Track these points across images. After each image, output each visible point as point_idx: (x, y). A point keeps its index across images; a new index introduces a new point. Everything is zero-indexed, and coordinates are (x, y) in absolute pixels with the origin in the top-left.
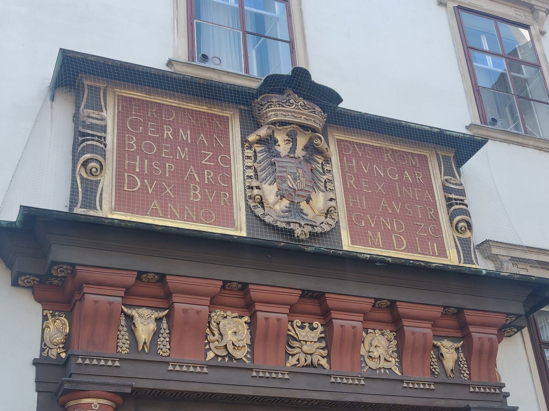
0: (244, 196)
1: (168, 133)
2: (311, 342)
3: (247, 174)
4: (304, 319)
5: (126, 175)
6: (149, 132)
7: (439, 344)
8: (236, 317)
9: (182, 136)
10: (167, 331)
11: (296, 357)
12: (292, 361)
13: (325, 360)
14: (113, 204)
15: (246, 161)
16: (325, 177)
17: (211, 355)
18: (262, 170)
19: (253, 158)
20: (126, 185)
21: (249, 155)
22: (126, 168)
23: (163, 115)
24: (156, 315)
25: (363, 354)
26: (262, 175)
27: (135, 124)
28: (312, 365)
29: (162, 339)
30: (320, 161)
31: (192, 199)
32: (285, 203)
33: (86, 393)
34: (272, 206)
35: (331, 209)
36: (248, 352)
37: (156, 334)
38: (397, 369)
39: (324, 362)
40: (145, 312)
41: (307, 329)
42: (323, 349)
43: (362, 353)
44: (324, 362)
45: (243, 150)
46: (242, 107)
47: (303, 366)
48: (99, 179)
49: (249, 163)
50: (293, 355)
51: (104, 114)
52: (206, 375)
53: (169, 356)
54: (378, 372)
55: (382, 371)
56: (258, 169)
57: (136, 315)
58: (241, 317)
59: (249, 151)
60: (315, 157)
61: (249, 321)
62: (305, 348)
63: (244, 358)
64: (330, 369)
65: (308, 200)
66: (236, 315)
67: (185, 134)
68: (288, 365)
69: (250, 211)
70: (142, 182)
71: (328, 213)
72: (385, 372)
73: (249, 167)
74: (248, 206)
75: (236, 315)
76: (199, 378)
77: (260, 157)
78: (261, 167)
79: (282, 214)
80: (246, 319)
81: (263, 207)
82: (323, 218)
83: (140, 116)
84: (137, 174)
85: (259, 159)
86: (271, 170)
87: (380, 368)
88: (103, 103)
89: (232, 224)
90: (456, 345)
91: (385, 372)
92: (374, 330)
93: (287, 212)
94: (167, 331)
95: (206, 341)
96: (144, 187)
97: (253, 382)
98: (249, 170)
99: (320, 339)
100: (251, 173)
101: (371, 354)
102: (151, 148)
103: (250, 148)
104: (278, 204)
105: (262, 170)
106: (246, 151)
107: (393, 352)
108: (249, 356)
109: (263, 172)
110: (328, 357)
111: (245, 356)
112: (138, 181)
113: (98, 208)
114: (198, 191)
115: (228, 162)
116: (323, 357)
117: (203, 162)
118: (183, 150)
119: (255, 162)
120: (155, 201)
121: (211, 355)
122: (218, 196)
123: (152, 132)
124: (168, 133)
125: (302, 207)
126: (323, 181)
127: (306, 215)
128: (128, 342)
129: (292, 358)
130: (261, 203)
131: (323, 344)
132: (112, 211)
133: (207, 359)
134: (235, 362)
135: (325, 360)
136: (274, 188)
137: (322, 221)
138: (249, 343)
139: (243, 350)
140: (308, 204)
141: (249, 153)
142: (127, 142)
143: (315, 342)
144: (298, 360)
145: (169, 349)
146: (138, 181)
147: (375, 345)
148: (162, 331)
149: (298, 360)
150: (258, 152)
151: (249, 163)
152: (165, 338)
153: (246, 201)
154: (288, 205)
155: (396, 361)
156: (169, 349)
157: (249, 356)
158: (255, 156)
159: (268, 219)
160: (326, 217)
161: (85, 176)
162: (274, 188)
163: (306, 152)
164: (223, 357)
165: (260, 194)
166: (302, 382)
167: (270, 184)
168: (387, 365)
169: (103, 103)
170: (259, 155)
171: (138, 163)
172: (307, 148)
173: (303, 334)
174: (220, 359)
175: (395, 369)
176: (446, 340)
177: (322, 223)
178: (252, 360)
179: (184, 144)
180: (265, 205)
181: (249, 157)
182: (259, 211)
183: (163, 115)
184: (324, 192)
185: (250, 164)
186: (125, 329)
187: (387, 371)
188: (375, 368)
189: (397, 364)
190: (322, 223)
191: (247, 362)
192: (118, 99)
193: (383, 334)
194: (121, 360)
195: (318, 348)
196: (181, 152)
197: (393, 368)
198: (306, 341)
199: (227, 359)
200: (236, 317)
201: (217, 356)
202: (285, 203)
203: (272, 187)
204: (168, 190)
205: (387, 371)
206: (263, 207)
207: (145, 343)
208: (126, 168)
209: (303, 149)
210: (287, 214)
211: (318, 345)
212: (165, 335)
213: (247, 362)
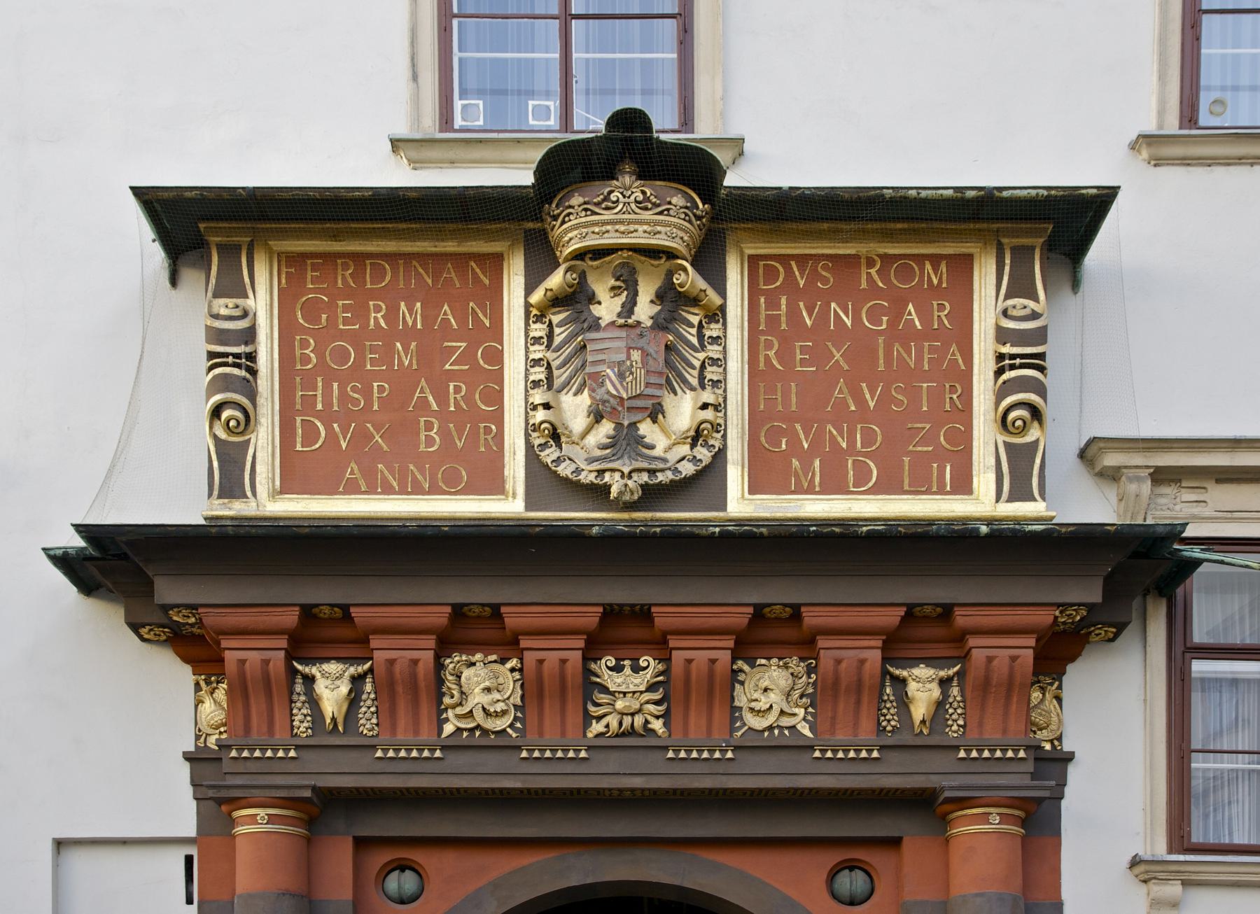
0: (523, 425)
1: (377, 318)
2: (634, 693)
3: (532, 378)
4: (620, 654)
5: (298, 419)
6: (340, 320)
7: (905, 673)
8: (495, 661)
9: (404, 318)
10: (372, 696)
11: (604, 721)
12: (597, 728)
13: (661, 721)
14: (278, 483)
15: (532, 348)
16: (702, 356)
17: (448, 729)
18: (559, 368)
19: (545, 340)
20: (299, 440)
21: (537, 334)
22: (298, 407)
23: (368, 279)
24: (352, 670)
25: (741, 705)
26: (560, 377)
27: (312, 311)
28: (632, 732)
29: (364, 709)
30: (695, 320)
31: (422, 448)
32: (606, 428)
33: (243, 802)
34: (576, 441)
35: (702, 426)
36: (516, 719)
37: (354, 700)
38: (807, 726)
39: (657, 725)
40: (333, 667)
41: (627, 671)
42: (657, 703)
43: (737, 703)
44: (657, 725)
45: (527, 324)
46: (530, 225)
47: (617, 736)
48: (247, 437)
49: (538, 352)
50: (599, 718)
51: (250, 302)
52: (441, 762)
53: (377, 735)
54: (766, 734)
55: (776, 732)
56: (554, 364)
57: (318, 675)
58: (503, 661)
59: (538, 325)
60: (683, 313)
61: (519, 665)
62: (620, 705)
63: (508, 730)
64: (670, 736)
65: (656, 413)
66: (494, 657)
67: (411, 310)
68: (590, 735)
69: (532, 455)
70: (329, 429)
71: (697, 437)
72: (781, 733)
73: (537, 362)
74: (529, 446)
75: (494, 657)
76: (429, 767)
77: (560, 335)
78: (562, 358)
79: (599, 453)
80: (514, 662)
81: (559, 446)
82: (685, 449)
83: (322, 291)
84: (318, 415)
85: (557, 340)
86: (577, 362)
87: (771, 728)
88: (247, 280)
89: (494, 484)
90: (942, 673)
91: (781, 733)
92: (769, 659)
93: (605, 447)
94: (372, 696)
95: (443, 707)
96: (331, 437)
97: (526, 768)
98: (537, 369)
99: (651, 688)
100: (539, 374)
101: (753, 705)
102: (343, 356)
103: (539, 319)
104: (593, 432)
105: (559, 368)
106: (533, 326)
107: (801, 697)
108: (518, 725)
109: (562, 370)
110: (666, 716)
111: (511, 726)
112: (321, 428)
113: (249, 494)
114: (435, 431)
115: (496, 357)
116: (657, 717)
117: (447, 367)
118: (406, 349)
119: (548, 347)
120: (353, 465)
121: (448, 729)
122: (474, 433)
123: (346, 321)
124: (377, 318)
125: (641, 432)
126: (697, 364)
127: (652, 447)
128: (309, 718)
129: (597, 723)
130: (555, 436)
131: (657, 696)
132: (275, 494)
133: (443, 736)
134: (493, 737)
135: (661, 721)
136: (585, 399)
137: (682, 455)
138: (519, 702)
139: (506, 717)
140: (654, 421)
141: (539, 330)
142: (298, 352)
143: (642, 692)
144: (607, 726)
145: (377, 725)
146: (321, 428)
147: (763, 687)
148: (364, 697)
149: (607, 726)
150: (557, 326)
151: (538, 352)
152: (369, 708)
153: (527, 435)
154: (612, 432)
155: (806, 713)
156: (377, 725)
157: (518, 725)
158: (550, 336)
159: (565, 470)
160: (693, 446)
161: (222, 435)
162: (585, 399)
163: (659, 307)
164: (472, 730)
165: (552, 419)
166: (612, 762)
167: (575, 394)
168: (786, 722)
169: (247, 280)
170: (557, 330)
171: (319, 392)
172: (662, 297)
173: (619, 681)
174: (465, 734)
175: (804, 727)
176: (922, 666)
177: (683, 459)
178: (522, 733)
179: (408, 334)
180: (563, 439)
181: (537, 340)
182: (549, 455)
183: (368, 279)
184: (693, 389)
185: (537, 356)
186: (303, 698)
187: (786, 732)
188: (761, 729)
189: (809, 718)
190: (683, 459)
191: (514, 735)
192: (279, 262)
193: (786, 667)
194: (297, 747)
195: (648, 702)
196: (402, 354)
197: (799, 727)
198: (625, 693)
199: (478, 733)
200: (495, 661)
201: (459, 730)
202: (607, 428)
203: (579, 397)
204: (377, 437)
205: (786, 732)
206: (559, 446)
207: (333, 719)
208: (298, 407)
209: (652, 302)
210: (608, 451)
211: (647, 696)
212: (369, 702)
213: (514, 735)
